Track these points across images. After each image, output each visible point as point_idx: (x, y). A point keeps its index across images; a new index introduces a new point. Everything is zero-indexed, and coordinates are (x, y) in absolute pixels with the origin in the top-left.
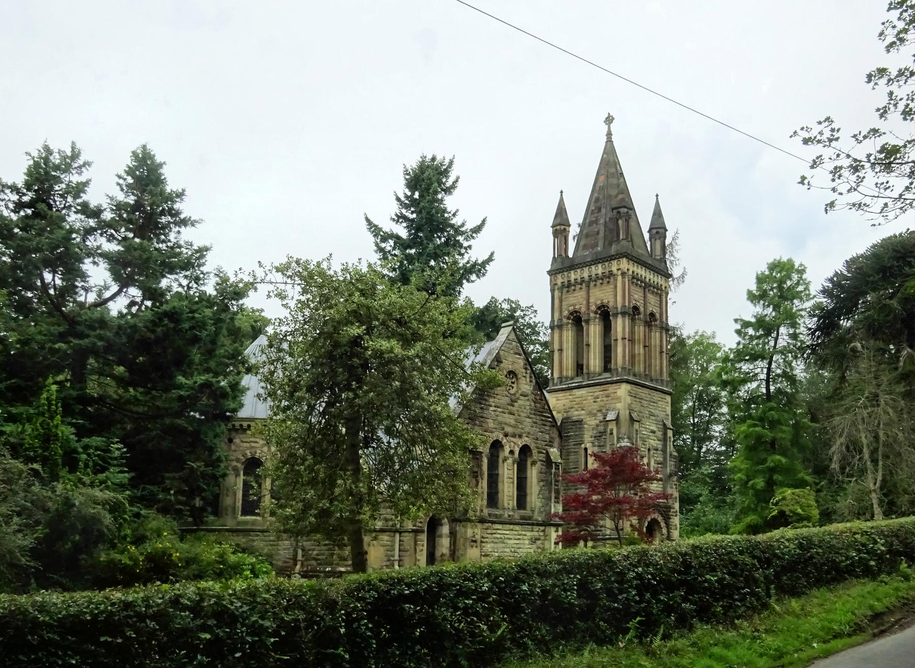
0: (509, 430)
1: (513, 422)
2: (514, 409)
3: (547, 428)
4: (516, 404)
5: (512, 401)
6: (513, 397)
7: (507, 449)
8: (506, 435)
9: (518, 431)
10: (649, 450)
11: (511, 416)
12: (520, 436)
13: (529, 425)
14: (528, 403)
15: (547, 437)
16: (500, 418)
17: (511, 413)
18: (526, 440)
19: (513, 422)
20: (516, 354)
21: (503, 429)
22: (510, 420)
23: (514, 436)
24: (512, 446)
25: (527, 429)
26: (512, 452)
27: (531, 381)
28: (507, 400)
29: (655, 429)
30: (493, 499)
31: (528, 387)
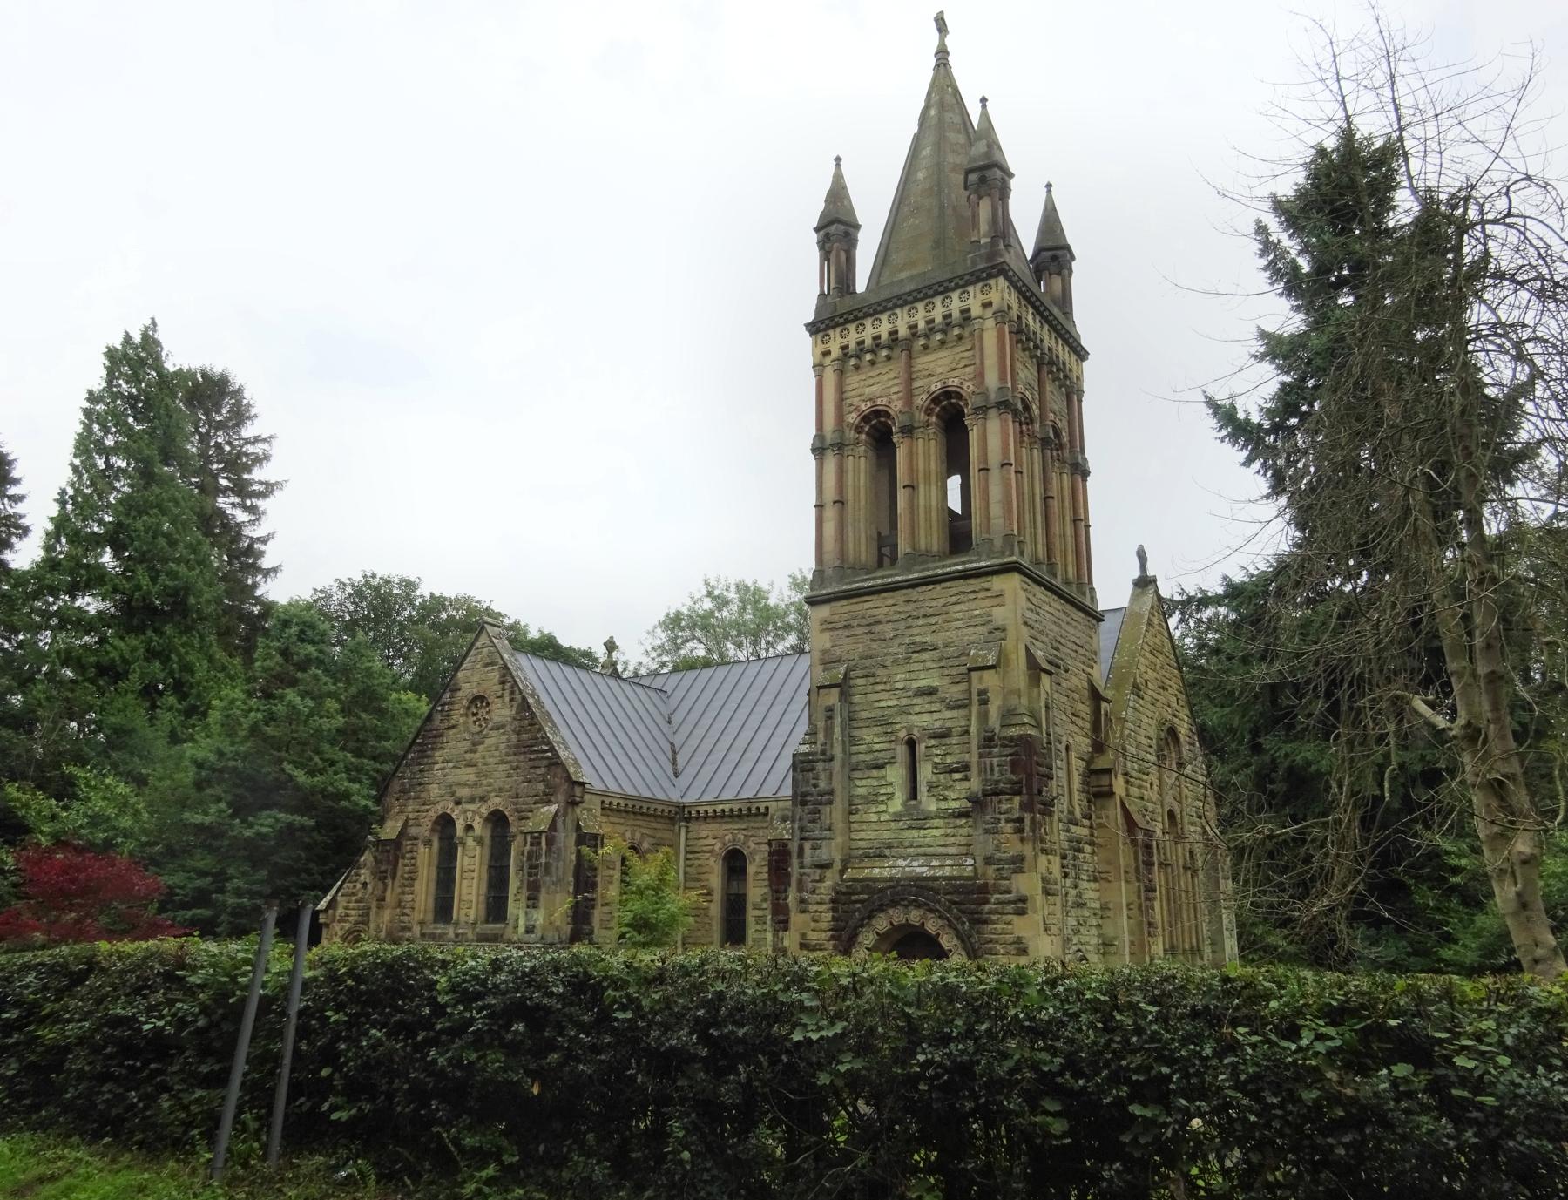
0: (464, 792)
1: (472, 778)
2: (478, 755)
3: (542, 771)
4: (481, 748)
5: (474, 744)
6: (477, 738)
7: (460, 825)
8: (458, 803)
9: (479, 792)
10: (911, 744)
11: (470, 770)
12: (483, 799)
13: (504, 775)
14: (504, 738)
15: (541, 786)
16: (450, 779)
17: (470, 764)
18: (495, 802)
19: (472, 778)
20: (487, 665)
21: (453, 794)
22: (468, 775)
23: (472, 800)
24: (471, 819)
25: (499, 784)
26: (469, 828)
27: (512, 700)
28: (466, 745)
29: (936, 683)
30: (443, 909)
31: (507, 712)
